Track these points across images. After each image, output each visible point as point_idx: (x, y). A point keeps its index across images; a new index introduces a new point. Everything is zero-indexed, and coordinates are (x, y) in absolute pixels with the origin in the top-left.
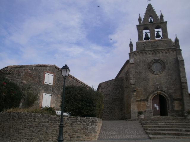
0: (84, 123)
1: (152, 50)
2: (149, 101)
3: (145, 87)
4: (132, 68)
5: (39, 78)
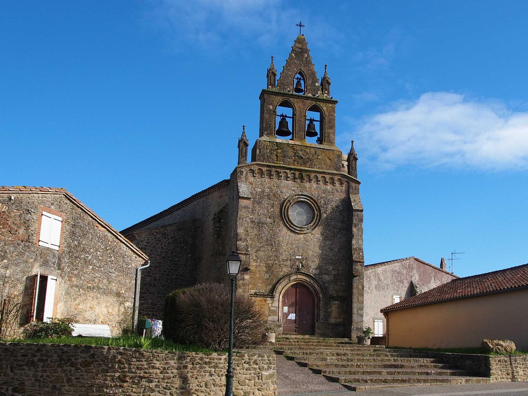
0: (255, 366)
1: (295, 170)
2: (276, 299)
3: (269, 262)
4: (243, 210)
5: (27, 228)
